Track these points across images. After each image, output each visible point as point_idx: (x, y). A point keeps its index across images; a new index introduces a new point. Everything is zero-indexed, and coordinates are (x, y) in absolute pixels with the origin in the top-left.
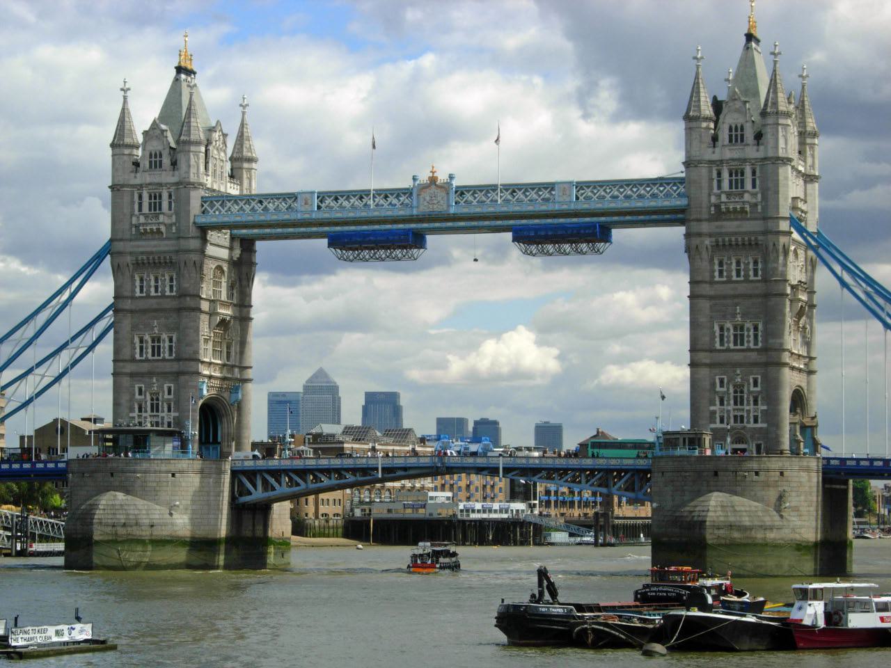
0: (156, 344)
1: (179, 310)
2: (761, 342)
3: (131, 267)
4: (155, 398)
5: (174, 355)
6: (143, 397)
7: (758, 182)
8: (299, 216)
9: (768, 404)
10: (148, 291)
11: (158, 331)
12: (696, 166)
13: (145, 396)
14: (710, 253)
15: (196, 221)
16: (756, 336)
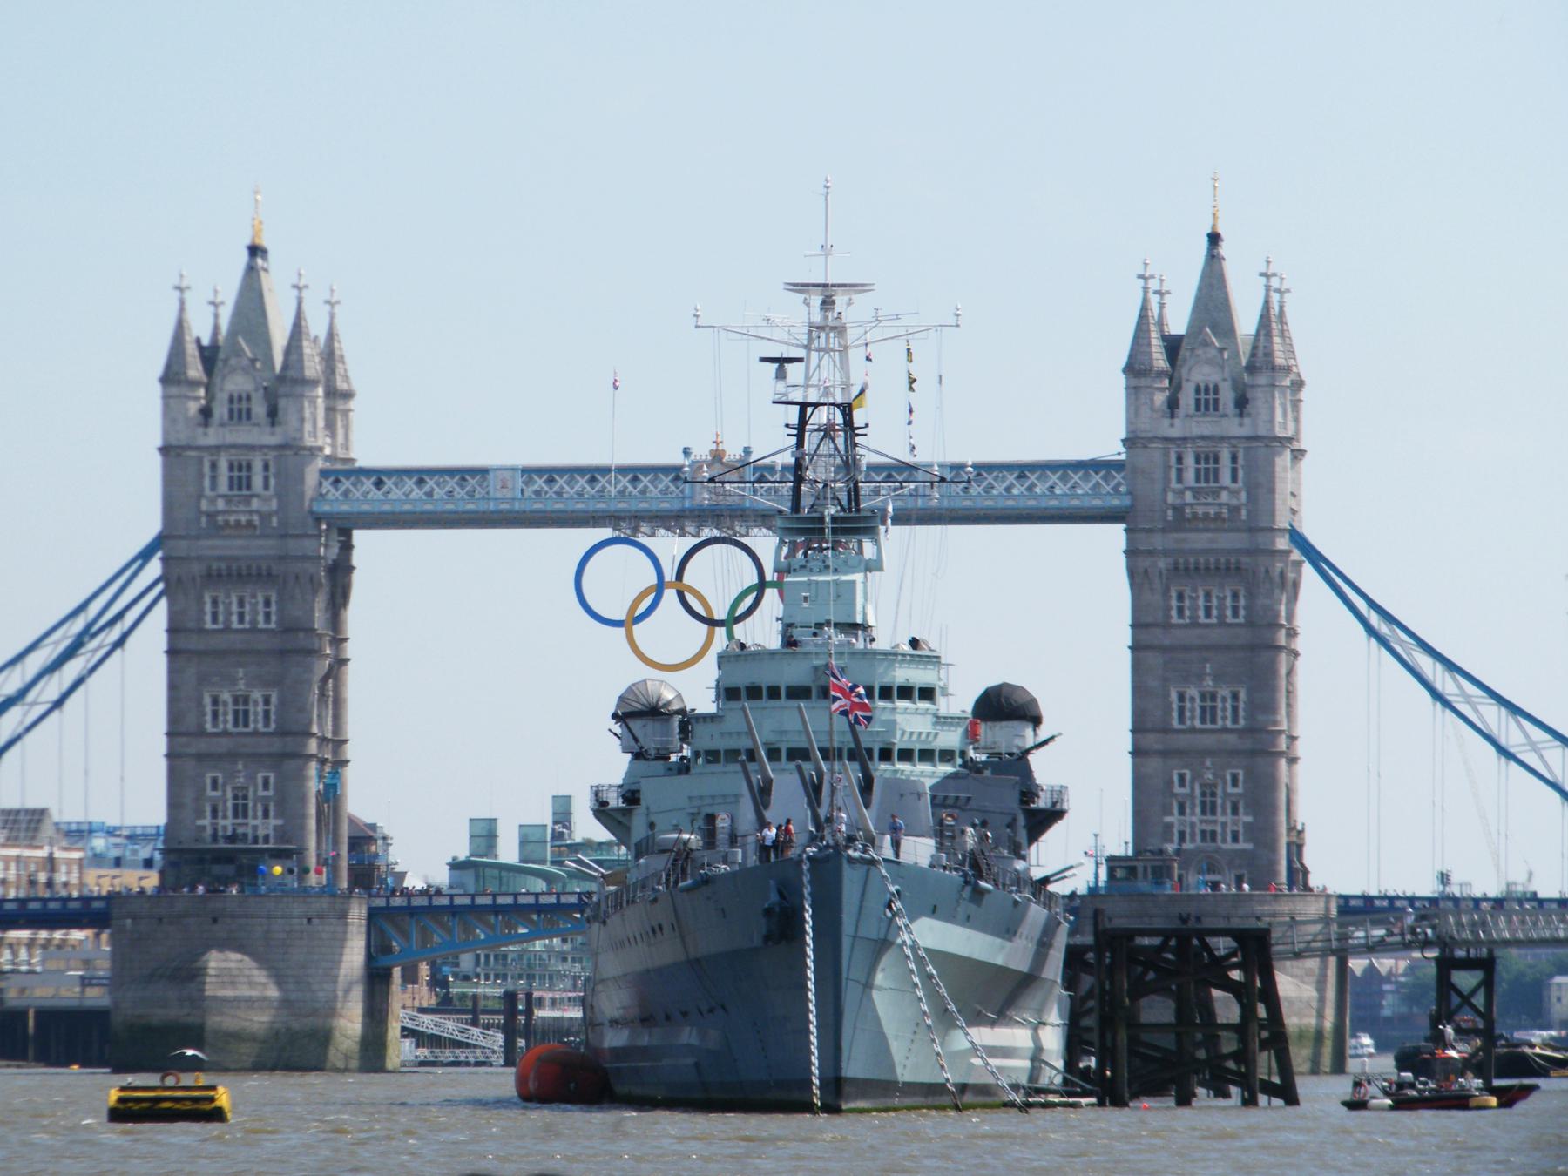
0: (241, 708)
1: (283, 653)
2: (1245, 719)
3: (198, 580)
4: (241, 796)
5: (273, 726)
6: (218, 793)
7: (1241, 474)
8: (492, 506)
9: (1255, 816)
10: (228, 621)
11: (247, 685)
12: (1146, 447)
13: (224, 791)
14: (1164, 581)
15: (315, 508)
16: (1235, 710)
